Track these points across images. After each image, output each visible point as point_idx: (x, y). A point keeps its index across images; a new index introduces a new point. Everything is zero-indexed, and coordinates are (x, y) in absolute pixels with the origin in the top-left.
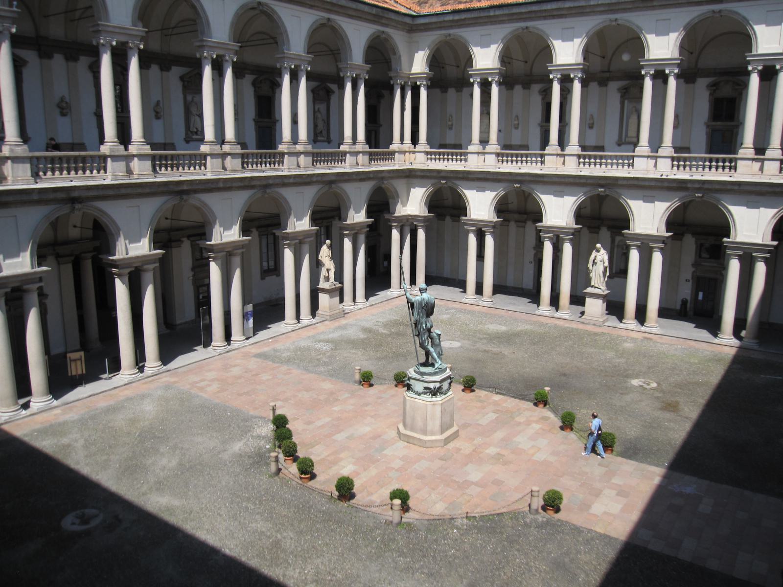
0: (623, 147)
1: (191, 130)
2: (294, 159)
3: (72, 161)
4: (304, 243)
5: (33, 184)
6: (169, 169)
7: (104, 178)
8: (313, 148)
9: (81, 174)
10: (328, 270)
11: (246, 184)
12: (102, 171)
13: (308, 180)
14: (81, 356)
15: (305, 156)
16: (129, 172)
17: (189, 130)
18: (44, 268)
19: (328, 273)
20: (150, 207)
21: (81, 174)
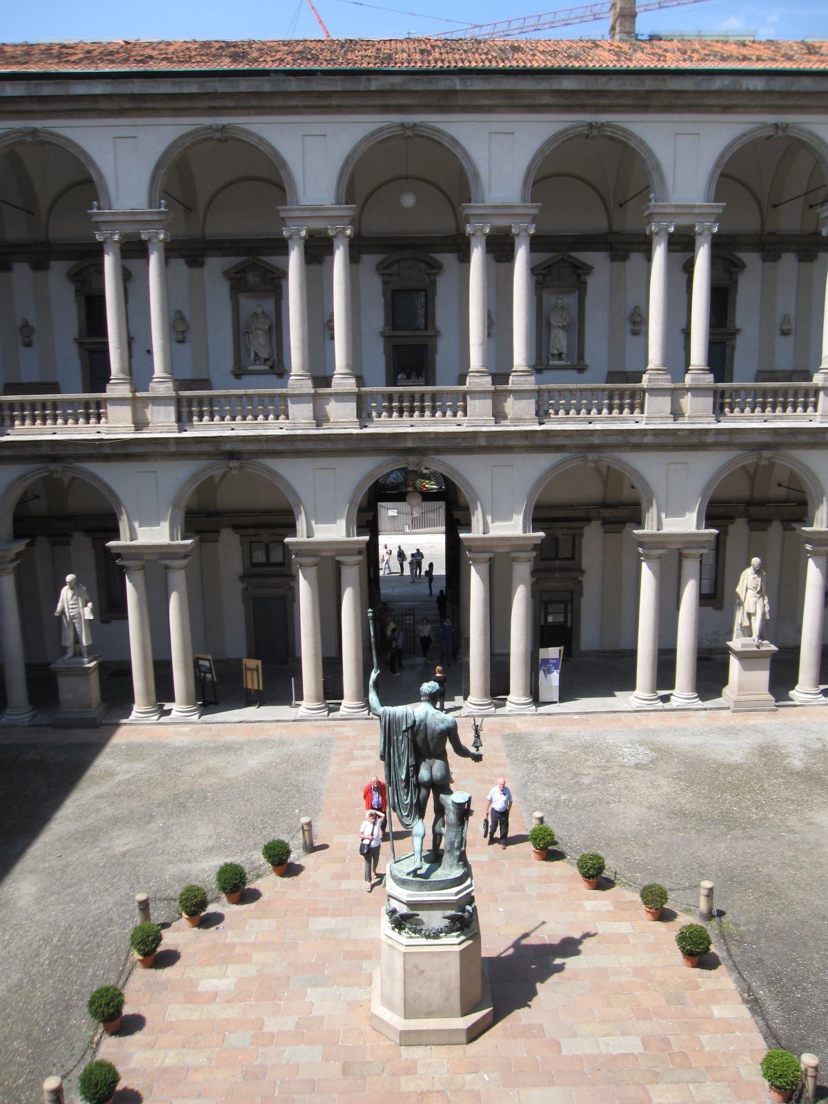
0: (245, 378)
1: (551, 351)
2: (665, 403)
3: (195, 403)
4: (687, 556)
5: (713, 423)
6: (395, 414)
7: (638, 419)
8: (716, 381)
9: (769, 412)
10: (750, 615)
11: (538, 442)
12: (637, 410)
13: (695, 440)
14: (257, 666)
15: (693, 396)
16: (677, 413)
17: (548, 352)
18: (189, 542)
19: (750, 619)
20: (530, 470)
21: (769, 412)
